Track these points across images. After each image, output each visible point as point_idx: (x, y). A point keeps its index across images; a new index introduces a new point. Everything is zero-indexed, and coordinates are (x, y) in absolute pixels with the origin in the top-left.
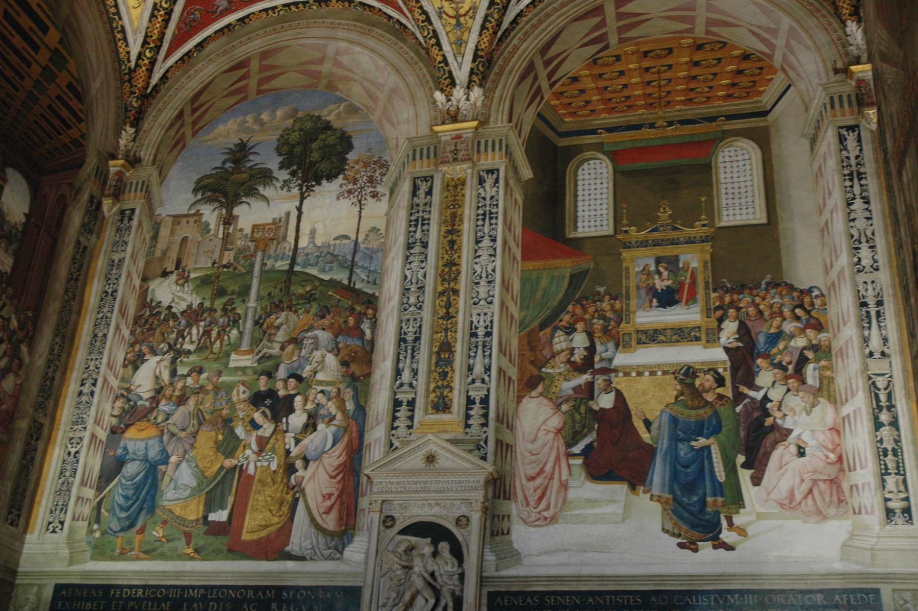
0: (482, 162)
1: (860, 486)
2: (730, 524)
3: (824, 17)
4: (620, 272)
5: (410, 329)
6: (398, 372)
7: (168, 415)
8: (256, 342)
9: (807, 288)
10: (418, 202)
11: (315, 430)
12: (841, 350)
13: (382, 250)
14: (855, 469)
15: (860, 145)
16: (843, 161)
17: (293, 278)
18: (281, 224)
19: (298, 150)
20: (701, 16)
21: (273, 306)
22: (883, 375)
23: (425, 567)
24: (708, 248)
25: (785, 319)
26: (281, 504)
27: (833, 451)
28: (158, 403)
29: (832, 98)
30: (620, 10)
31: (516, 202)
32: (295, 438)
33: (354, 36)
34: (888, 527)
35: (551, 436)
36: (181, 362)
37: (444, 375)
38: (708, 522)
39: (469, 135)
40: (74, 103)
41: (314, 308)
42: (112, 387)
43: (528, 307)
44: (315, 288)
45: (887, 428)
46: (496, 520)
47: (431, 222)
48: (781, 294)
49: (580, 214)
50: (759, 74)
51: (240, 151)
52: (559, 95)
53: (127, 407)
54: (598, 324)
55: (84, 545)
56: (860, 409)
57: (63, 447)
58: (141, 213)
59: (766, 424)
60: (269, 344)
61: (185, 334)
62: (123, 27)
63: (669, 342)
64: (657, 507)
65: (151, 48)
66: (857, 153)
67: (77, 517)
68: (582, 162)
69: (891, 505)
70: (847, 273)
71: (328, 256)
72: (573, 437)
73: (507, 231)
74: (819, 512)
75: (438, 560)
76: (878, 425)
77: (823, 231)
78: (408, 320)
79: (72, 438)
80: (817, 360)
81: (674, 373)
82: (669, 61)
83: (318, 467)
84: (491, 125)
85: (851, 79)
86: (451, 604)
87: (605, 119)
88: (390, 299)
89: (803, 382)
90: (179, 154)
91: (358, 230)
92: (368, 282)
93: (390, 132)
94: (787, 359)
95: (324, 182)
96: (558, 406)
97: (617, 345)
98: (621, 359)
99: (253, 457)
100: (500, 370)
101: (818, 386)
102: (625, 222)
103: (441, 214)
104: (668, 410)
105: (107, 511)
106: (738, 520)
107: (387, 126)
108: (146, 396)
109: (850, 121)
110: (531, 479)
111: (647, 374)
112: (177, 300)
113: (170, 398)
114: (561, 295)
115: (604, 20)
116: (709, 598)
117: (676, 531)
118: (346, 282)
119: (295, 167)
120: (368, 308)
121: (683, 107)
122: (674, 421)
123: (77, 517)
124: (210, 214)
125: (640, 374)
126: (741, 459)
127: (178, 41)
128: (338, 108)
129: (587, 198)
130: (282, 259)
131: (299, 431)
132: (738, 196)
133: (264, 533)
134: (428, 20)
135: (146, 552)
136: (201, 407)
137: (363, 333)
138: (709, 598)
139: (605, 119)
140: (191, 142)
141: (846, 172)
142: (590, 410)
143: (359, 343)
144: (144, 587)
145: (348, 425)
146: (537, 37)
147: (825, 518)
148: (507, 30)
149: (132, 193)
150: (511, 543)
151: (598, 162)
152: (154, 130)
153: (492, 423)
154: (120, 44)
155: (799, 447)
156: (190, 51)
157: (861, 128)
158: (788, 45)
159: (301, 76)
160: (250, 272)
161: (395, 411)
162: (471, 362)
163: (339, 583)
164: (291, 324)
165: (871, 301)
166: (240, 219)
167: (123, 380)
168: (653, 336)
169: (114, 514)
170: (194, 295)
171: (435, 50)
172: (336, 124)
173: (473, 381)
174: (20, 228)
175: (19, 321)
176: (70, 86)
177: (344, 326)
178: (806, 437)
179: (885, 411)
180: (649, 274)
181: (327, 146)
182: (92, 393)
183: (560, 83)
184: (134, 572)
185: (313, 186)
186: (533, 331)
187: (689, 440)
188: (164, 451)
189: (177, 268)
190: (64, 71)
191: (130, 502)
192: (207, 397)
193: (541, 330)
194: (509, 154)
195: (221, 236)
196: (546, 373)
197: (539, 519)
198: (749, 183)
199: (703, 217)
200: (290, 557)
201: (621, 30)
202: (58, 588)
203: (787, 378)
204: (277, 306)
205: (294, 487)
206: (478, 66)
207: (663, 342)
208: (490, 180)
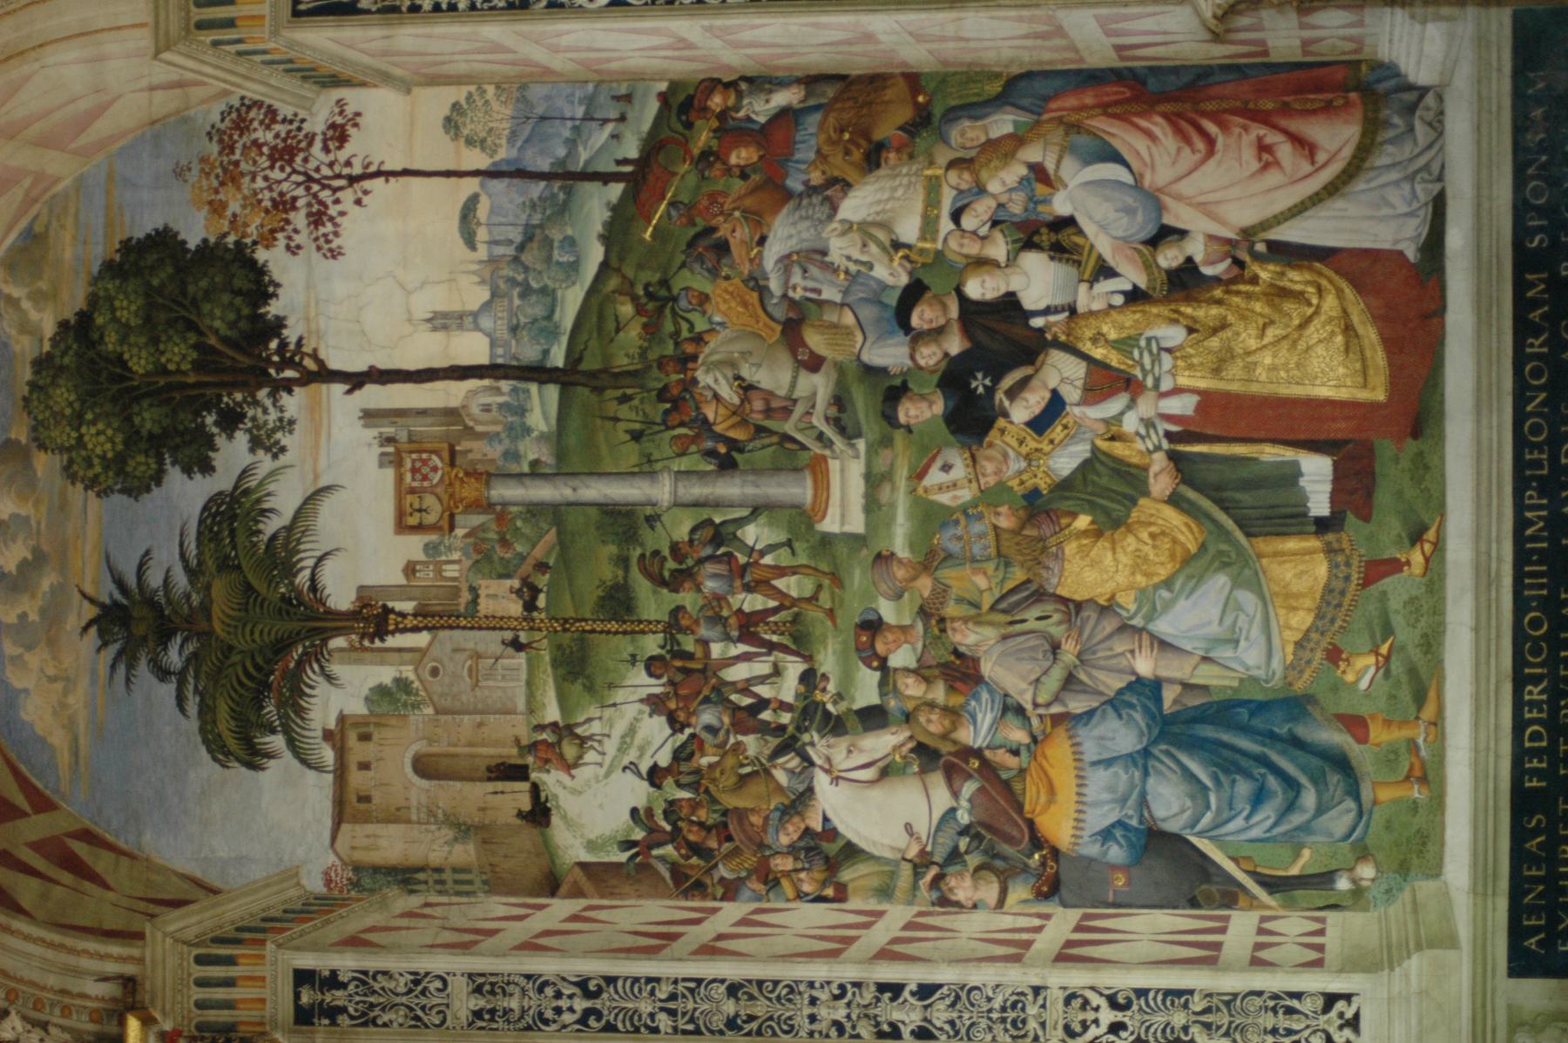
7: (1006, 709)
11: (1070, 222)
13: (523, 87)
17: (590, 363)
18: (403, 436)
19: (148, 418)
21: (675, 418)
26: (1285, 293)
36: (839, 697)
42: (907, 927)
44: (627, 289)
53: (973, 860)
55: (1397, 910)
58: (315, 947)
60: (799, 410)
61: (747, 701)
67: (1313, 955)
79: (1067, 1029)
83: (1179, 198)
90: (110, 847)
91: (448, 174)
92: (622, 118)
93: (127, 114)
95: (273, 309)
99: (1146, 406)
105: (1297, 855)
108: (942, 798)
112: (632, 756)
113: (952, 713)
118: (616, 190)
119: (210, 419)
123: (1313, 955)
130: (522, 411)
131: (1072, 271)
133: (1370, 334)
135: (1420, 698)
136: (987, 602)
137: (785, 113)
140: (75, 811)
144: (1520, 681)
145: (1060, 120)
160: (555, 513)
164: (736, 348)
166: (370, 581)
167: (885, 892)
169: (1305, 828)
170: (620, 696)
172: (74, 299)
177: (756, 178)
181: (148, 319)
182: (926, 991)
184: (1476, 725)
185: (283, 345)
188: (1116, 703)
191: (1273, 782)
195: (422, 639)
200: (1434, 244)
202: (1522, 964)
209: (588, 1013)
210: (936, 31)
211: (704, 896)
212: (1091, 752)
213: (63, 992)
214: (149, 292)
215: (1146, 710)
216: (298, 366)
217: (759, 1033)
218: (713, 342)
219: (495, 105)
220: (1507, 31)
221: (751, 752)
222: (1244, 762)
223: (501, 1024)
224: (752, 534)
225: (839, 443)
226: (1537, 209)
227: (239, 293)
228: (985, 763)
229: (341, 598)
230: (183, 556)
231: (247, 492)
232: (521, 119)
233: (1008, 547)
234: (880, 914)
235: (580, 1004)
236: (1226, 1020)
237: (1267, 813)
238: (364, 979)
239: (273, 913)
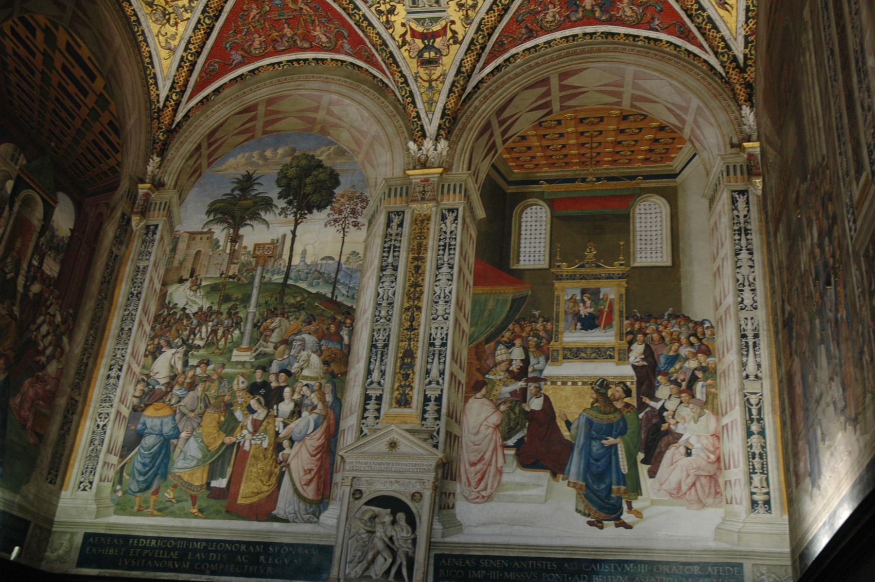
0: (445, 202)
1: (733, 482)
2: (630, 507)
3: (725, 100)
4: (551, 299)
5: (381, 337)
6: (369, 372)
8: (254, 341)
11: (300, 416)
12: (724, 372)
14: (729, 468)
17: (287, 290)
19: (295, 183)
20: (628, 92)
22: (756, 393)
23: (385, 532)
24: (624, 283)
25: (681, 345)
26: (270, 475)
27: (713, 453)
28: (172, 388)
29: (728, 167)
31: (471, 236)
32: (283, 422)
33: (343, 90)
34: (752, 515)
35: (490, 430)
36: (192, 355)
37: (406, 376)
40: (113, 137)
41: (303, 316)
43: (477, 324)
44: (304, 299)
46: (443, 496)
47: (401, 250)
49: (522, 250)
50: (672, 143)
52: (510, 150)
54: (532, 341)
55: (108, 502)
56: (736, 420)
57: (93, 421)
58: (163, 229)
59: (662, 429)
60: (265, 344)
62: (155, 74)
63: (589, 359)
64: (573, 492)
65: (177, 93)
66: (746, 213)
68: (526, 207)
69: (756, 497)
70: (732, 310)
71: (316, 273)
72: (509, 432)
74: (700, 501)
75: (395, 527)
76: (749, 434)
77: (715, 275)
78: (379, 330)
80: (705, 379)
81: (591, 384)
82: (599, 127)
84: (454, 172)
86: (405, 563)
87: (546, 172)
88: (365, 311)
89: (693, 396)
92: (348, 297)
93: (371, 173)
94: (682, 377)
95: (315, 211)
96: (497, 407)
97: (547, 359)
98: (550, 371)
99: (248, 436)
100: (452, 375)
101: (704, 400)
102: (558, 258)
103: (409, 243)
104: (585, 414)
105: (128, 475)
106: (635, 505)
107: (368, 167)
108: (162, 381)
110: (473, 464)
111: (570, 383)
112: (190, 303)
113: (182, 385)
114: (504, 315)
116: (610, 566)
117: (587, 512)
120: (346, 318)
121: (609, 166)
122: (590, 423)
124: (220, 233)
125: (564, 383)
126: (641, 456)
127: (200, 86)
128: (329, 150)
130: (278, 273)
132: (649, 242)
133: (255, 499)
134: (406, 82)
135: (159, 510)
136: (207, 393)
137: (342, 339)
138: (610, 566)
139: (546, 172)
140: (206, 172)
141: (736, 228)
142: (523, 411)
143: (338, 346)
145: (327, 414)
146: (494, 100)
148: (470, 93)
149: (157, 211)
150: (454, 515)
151: (539, 207)
152: (177, 158)
153: (444, 418)
155: (687, 449)
156: (208, 95)
157: (750, 193)
158: (695, 121)
160: (251, 283)
161: (366, 404)
162: (429, 367)
163: (316, 541)
164: (283, 328)
165: (750, 334)
167: (144, 367)
168: (576, 353)
169: (134, 478)
171: (410, 108)
172: (327, 163)
173: (430, 383)
174: (66, 242)
175: (62, 317)
176: (110, 123)
178: (693, 441)
179: (755, 423)
180: (575, 302)
182: (118, 377)
185: (306, 214)
186: (480, 343)
187: (600, 439)
188: (176, 427)
189: (191, 276)
190: (107, 112)
191: (147, 468)
192: (212, 385)
194: (467, 197)
195: (228, 251)
196: (489, 379)
197: (478, 498)
200: (276, 519)
201: (563, 99)
202: (87, 536)
203: (681, 392)
204: (272, 312)
207: (584, 358)
208: (450, 217)
224: (237, 332)
225: (255, 354)
235: (135, 292)
238: (153, 241)
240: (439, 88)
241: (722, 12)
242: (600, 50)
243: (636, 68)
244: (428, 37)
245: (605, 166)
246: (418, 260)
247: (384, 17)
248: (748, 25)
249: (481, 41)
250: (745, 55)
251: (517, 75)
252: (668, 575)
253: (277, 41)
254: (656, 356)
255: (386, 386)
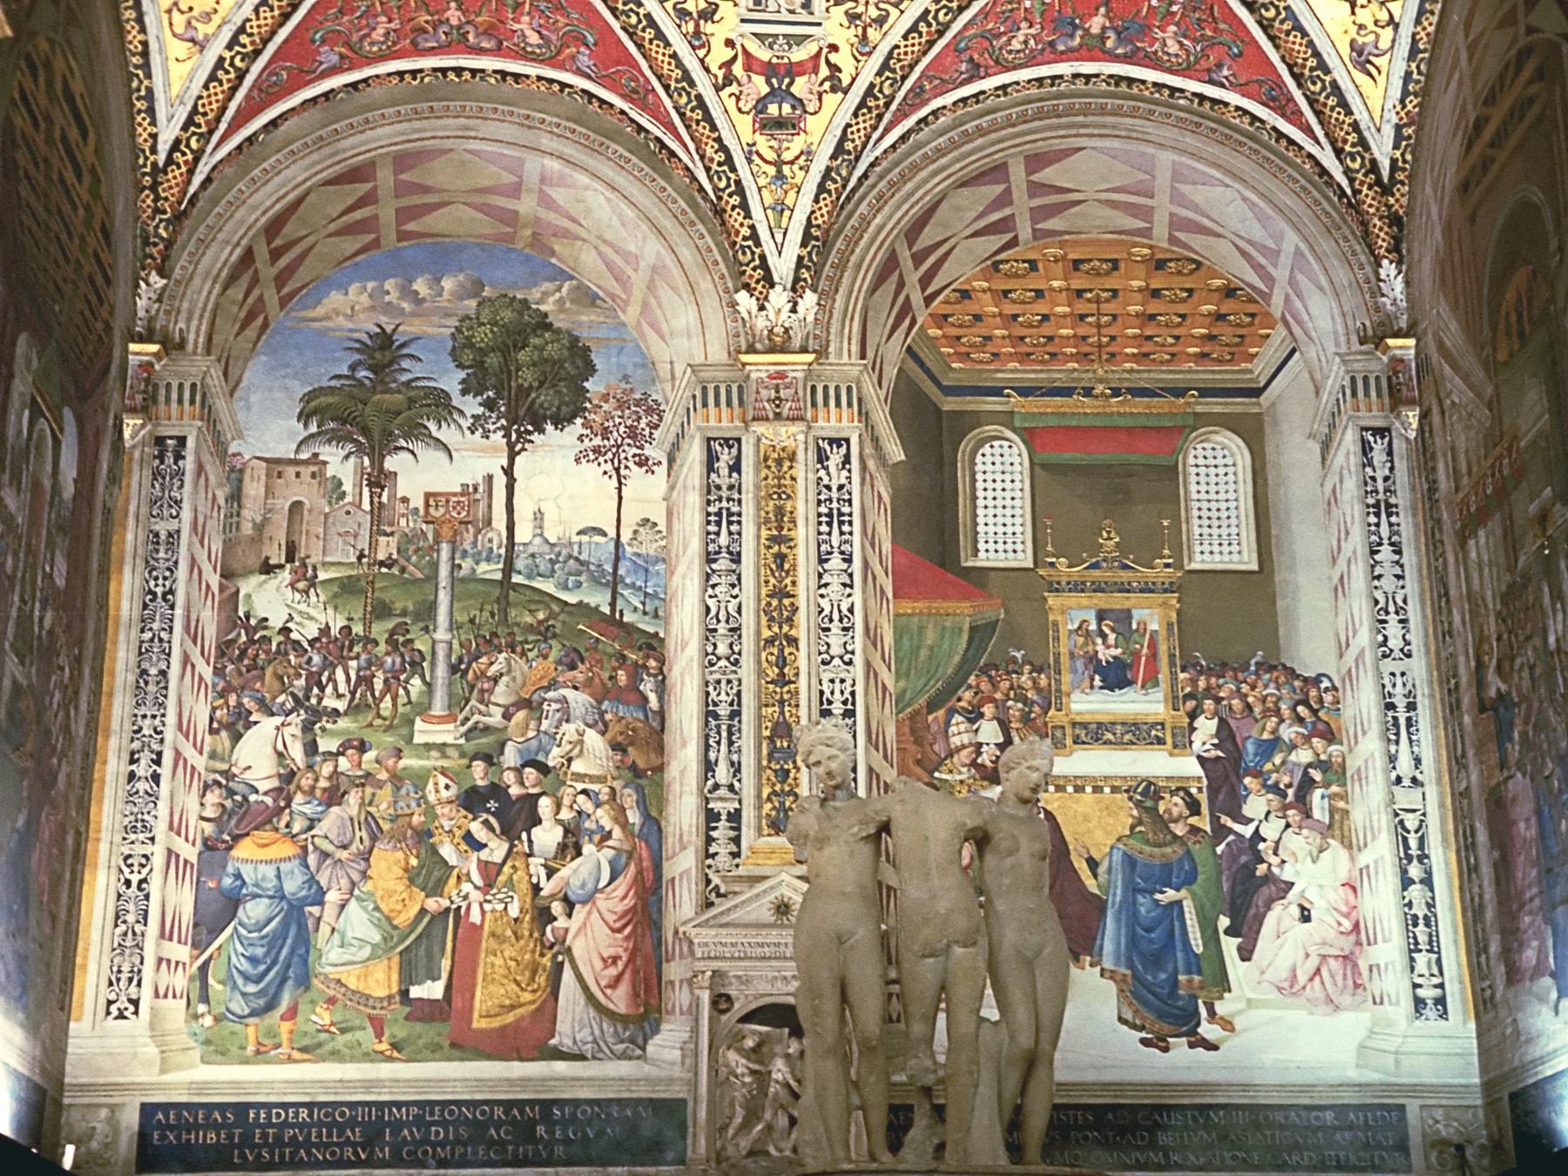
0: (821, 423)
4: (1045, 630)
5: (723, 697)
6: (709, 767)
7: (312, 820)
8: (457, 703)
9: (1313, 675)
10: (718, 481)
11: (579, 854)
12: (1359, 770)
13: (664, 560)
15: (1392, 461)
16: (1366, 484)
18: (478, 496)
19: (493, 360)
20: (1163, 209)
21: (481, 641)
22: (1414, 811)
24: (1174, 602)
25: (1282, 721)
26: (534, 972)
27: (1347, 916)
29: (1353, 379)
30: (1035, 177)
31: (880, 497)
33: (570, 150)
34: (1417, 1023)
36: (323, 729)
38: (1184, 1010)
39: (800, 375)
42: (193, 768)
43: (908, 675)
44: (552, 615)
45: (1418, 886)
47: (743, 519)
48: (1276, 682)
49: (981, 528)
50: (1251, 324)
51: (382, 348)
52: (941, 319)
53: (228, 803)
57: (114, 872)
59: (1258, 873)
60: (482, 708)
61: (324, 680)
62: (150, 90)
63: (1120, 744)
64: (1111, 987)
65: (201, 135)
66: (1387, 472)
68: (981, 443)
69: (1421, 992)
73: (868, 545)
76: (1406, 882)
77: (1336, 589)
78: (718, 682)
79: (130, 856)
80: (1327, 785)
81: (1127, 791)
82: (1111, 283)
83: (589, 913)
84: (832, 359)
85: (1384, 353)
88: (684, 645)
92: (645, 613)
93: (658, 349)
94: (1286, 780)
95: (549, 427)
99: (476, 896)
100: (870, 770)
102: (1049, 548)
103: (758, 508)
106: (1221, 1008)
107: (652, 336)
108: (263, 786)
109: (1379, 423)
111: (1089, 789)
112: (297, 618)
114: (957, 659)
115: (1008, 191)
116: (1185, 1116)
117: (1138, 1022)
118: (606, 610)
120: (647, 657)
122: (1130, 862)
123: (162, 992)
124: (341, 464)
125: (1079, 789)
126: (1224, 922)
128: (559, 289)
129: (990, 503)
130: (488, 560)
131: (552, 855)
132: (1215, 523)
133: (510, 1018)
134: (729, 161)
135: (303, 1050)
136: (372, 809)
137: (646, 699)
141: (1371, 501)
145: (634, 848)
146: (899, 207)
147: (1337, 1008)
149: (174, 405)
151: (1006, 444)
152: (197, 281)
154: (139, 119)
155: (1303, 908)
156: (255, 134)
158: (1292, 282)
159: (480, 215)
160: (433, 577)
163: (642, 1092)
164: (518, 674)
165: (1401, 703)
167: (213, 756)
168: (1095, 733)
169: (235, 986)
170: (330, 611)
171: (736, 217)
172: (559, 322)
177: (609, 684)
179: (1415, 862)
180: (1088, 634)
181: (546, 361)
182: (156, 778)
183: (941, 298)
185: (530, 433)
186: (917, 712)
187: (1152, 892)
188: (312, 880)
189: (290, 558)
191: (262, 968)
193: (929, 713)
194: (864, 415)
195: (366, 506)
196: (940, 780)
198: (1232, 505)
199: (1166, 552)
200: (558, 1055)
201: (1038, 214)
202: (147, 1110)
203: (1285, 808)
204: (489, 642)
205: (552, 946)
206: (810, 253)
208: (835, 459)
209: (154, 594)
210: (686, 781)
211: (216, 658)
212: (284, 867)
213: (179, 312)
214: (561, 362)
215: (306, 897)
216: (518, 441)
217: (138, 687)
218: (522, 662)
219: (655, 545)
220: (675, 1096)
221: (296, 683)
222: (273, 953)
223: (150, 547)
224: (416, 681)
225: (463, 729)
226: (575, 1113)
227: (558, 409)
228: (283, 809)
229: (390, 463)
230: (418, 379)
231: (451, 413)
232: (647, 558)
233: (401, 821)
234: (201, 753)
235: (159, 590)
236: (128, 944)
237: (245, 965)
238: (180, 474)
239: (218, 427)
240: (798, 180)
241: (1360, 78)
242: (1102, 110)
243: (1175, 157)
244: (780, 74)
245: (1128, 365)
246: (779, 541)
247: (691, 25)
248: (1404, 107)
249: (887, 91)
250: (1394, 161)
251: (940, 152)
252: (1282, 1127)
253: (425, 31)
254: (1238, 740)
255: (745, 793)
